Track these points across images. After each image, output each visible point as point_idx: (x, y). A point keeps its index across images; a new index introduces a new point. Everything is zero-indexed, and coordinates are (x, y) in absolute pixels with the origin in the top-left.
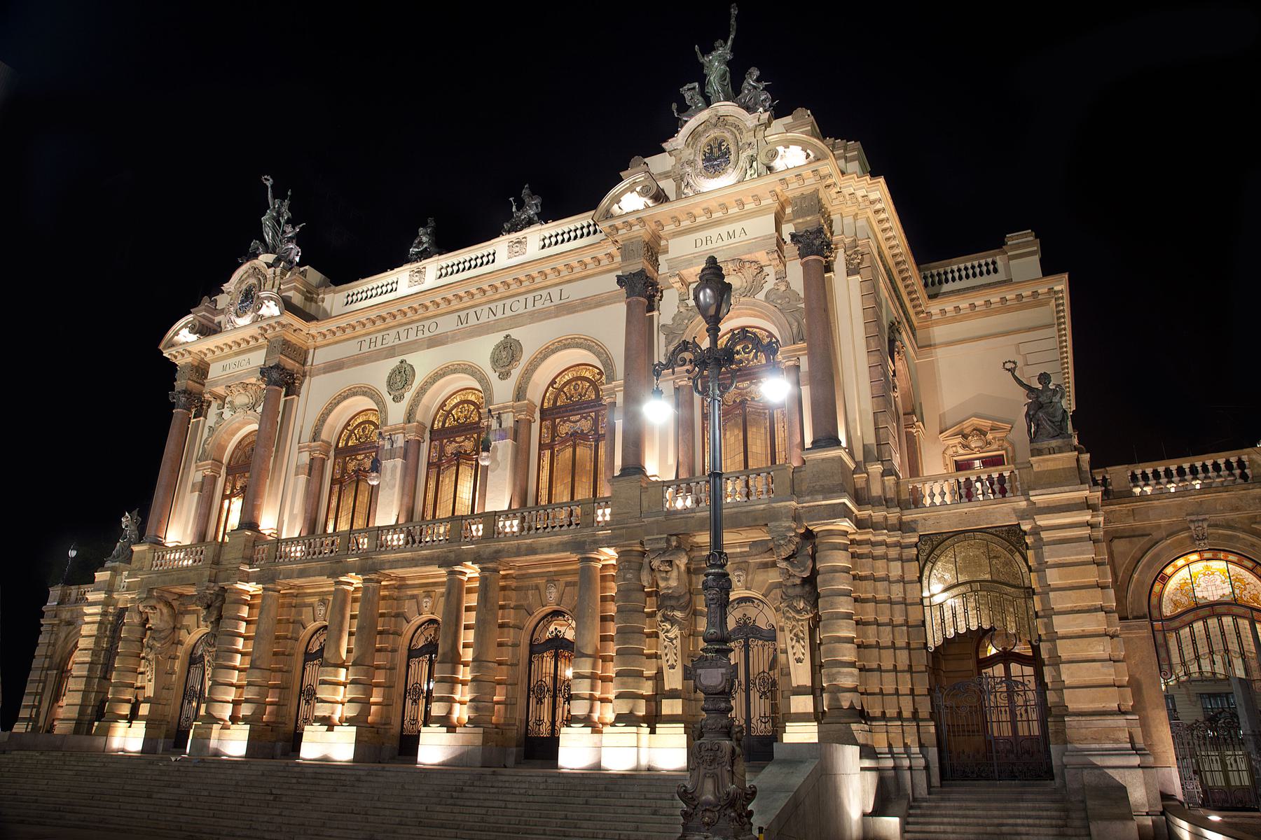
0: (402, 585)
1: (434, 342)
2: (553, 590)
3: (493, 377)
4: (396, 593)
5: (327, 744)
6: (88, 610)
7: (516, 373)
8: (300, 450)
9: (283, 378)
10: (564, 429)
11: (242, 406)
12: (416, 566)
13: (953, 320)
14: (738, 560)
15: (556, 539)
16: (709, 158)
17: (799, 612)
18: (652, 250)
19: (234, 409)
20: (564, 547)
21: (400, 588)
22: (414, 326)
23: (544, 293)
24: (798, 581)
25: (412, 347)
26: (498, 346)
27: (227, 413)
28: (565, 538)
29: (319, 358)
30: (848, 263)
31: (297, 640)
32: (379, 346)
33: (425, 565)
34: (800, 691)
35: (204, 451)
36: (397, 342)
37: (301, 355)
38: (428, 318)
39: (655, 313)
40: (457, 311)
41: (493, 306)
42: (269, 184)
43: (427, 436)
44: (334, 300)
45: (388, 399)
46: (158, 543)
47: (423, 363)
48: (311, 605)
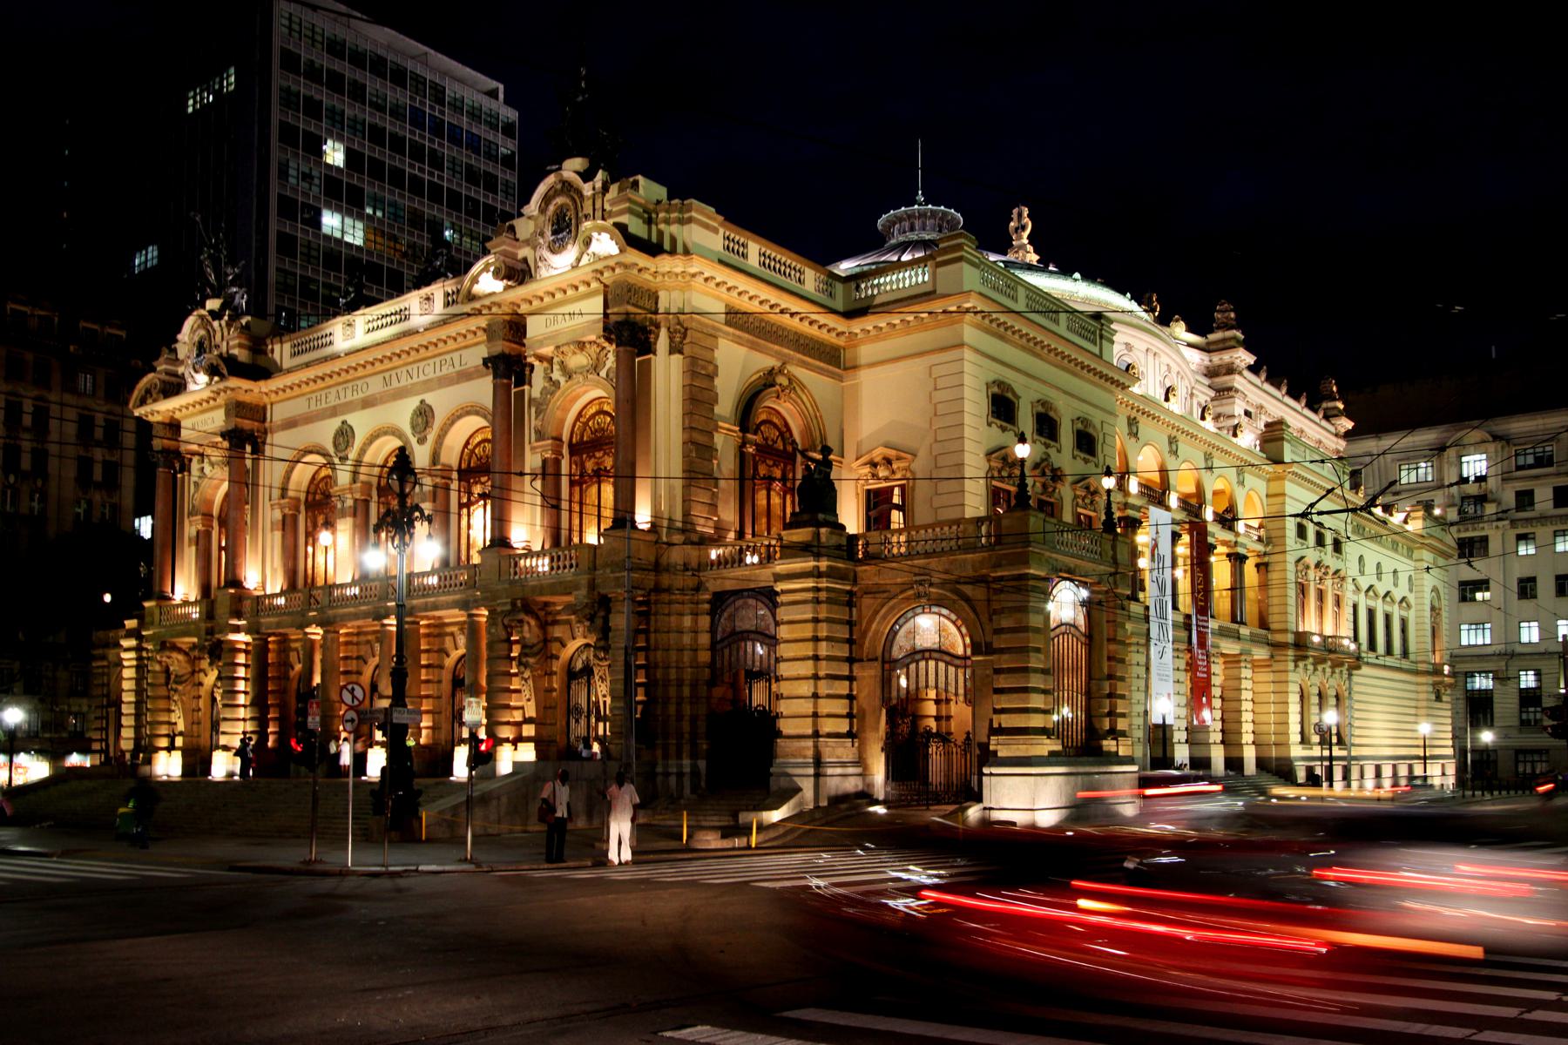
1: (367, 403)
3: (413, 440)
6: (124, 655)
9: (245, 437)
18: (516, 327)
19: (212, 464)
23: (448, 357)
25: (349, 407)
27: (207, 469)
28: (457, 597)
29: (278, 414)
30: (671, 339)
37: (258, 412)
39: (526, 387)
43: (374, 493)
44: (281, 352)
46: (164, 598)
47: (363, 424)
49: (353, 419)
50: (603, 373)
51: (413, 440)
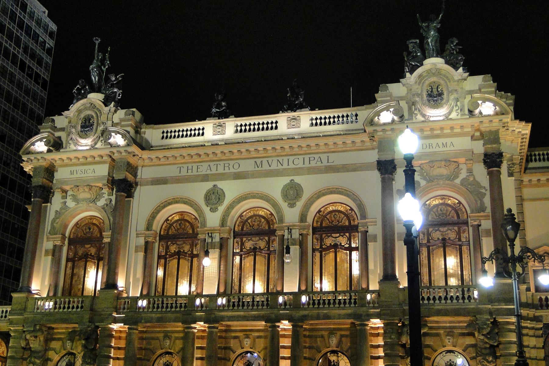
0: (228, 330)
1: (238, 176)
2: (334, 339)
3: (284, 205)
4: (223, 334)
7: (300, 204)
8: (138, 235)
10: (329, 241)
11: (84, 200)
12: (248, 320)
13: (536, 186)
14: (448, 330)
15: (343, 312)
16: (430, 95)
17: (489, 362)
20: (349, 316)
21: (226, 331)
22: (222, 163)
23: (316, 156)
24: (488, 346)
26: (285, 186)
28: (349, 311)
29: (144, 174)
30: (509, 168)
31: (148, 360)
32: (195, 173)
33: (254, 320)
35: (53, 227)
36: (209, 172)
38: (232, 160)
41: (280, 159)
42: (97, 42)
45: (206, 210)
47: (231, 189)
49: (221, 184)
50: (458, 181)
51: (284, 205)
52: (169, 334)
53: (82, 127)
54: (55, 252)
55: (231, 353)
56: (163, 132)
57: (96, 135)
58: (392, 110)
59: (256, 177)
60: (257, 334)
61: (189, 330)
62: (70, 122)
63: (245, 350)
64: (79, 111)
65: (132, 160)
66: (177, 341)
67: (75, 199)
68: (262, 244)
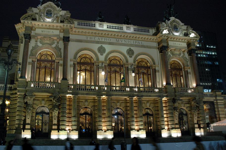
1: (110, 44)
3: (128, 57)
5: (105, 134)
7: (133, 57)
8: (71, 60)
10: (141, 71)
20: (157, 96)
22: (104, 38)
23: (138, 41)
32: (93, 40)
34: (196, 124)
36: (99, 40)
40: (116, 38)
41: (125, 40)
45: (99, 54)
47: (108, 48)
48: (82, 102)
52: (87, 100)
53: (46, 13)
54: (33, 63)
55: (113, 108)
56: (78, 23)
57: (54, 18)
58: (167, 30)
59: (117, 45)
60: (122, 101)
61: (100, 99)
62: (40, 11)
63: (117, 107)
64: (45, 8)
65: (70, 30)
66: (90, 103)
67: (41, 43)
68: (118, 70)
